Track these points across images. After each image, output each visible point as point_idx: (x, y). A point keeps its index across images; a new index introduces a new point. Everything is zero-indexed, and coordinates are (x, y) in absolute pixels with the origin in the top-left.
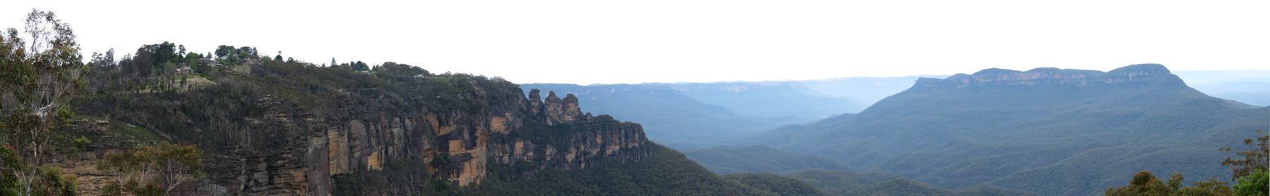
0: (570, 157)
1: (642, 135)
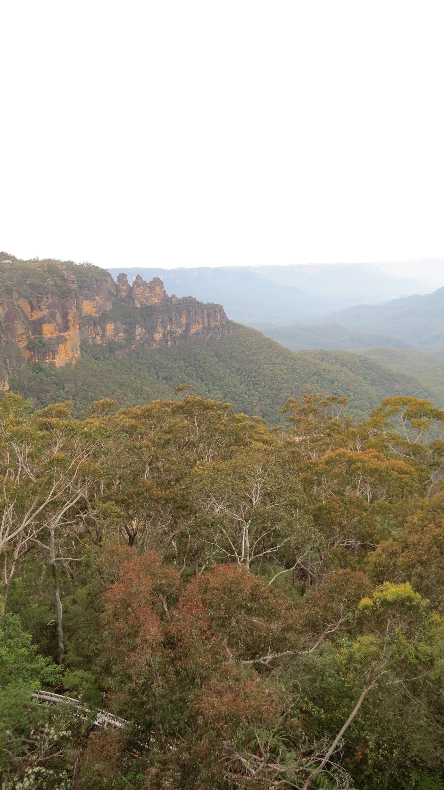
0: (158, 336)
1: (223, 315)
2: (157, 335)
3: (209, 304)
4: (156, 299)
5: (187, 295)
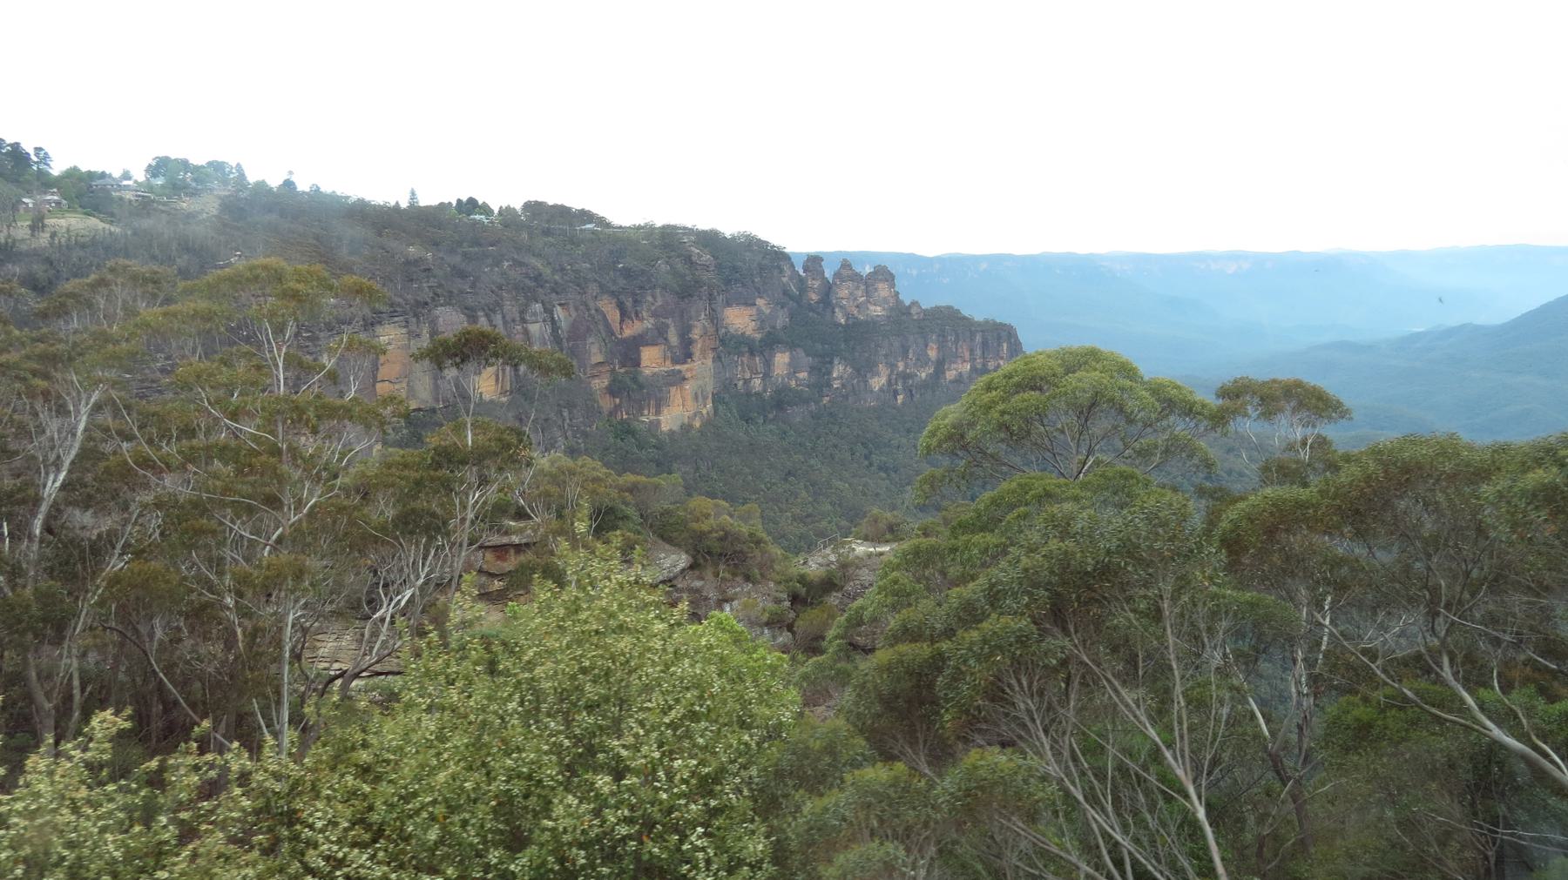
0: (878, 382)
3: (987, 322)
5: (943, 301)
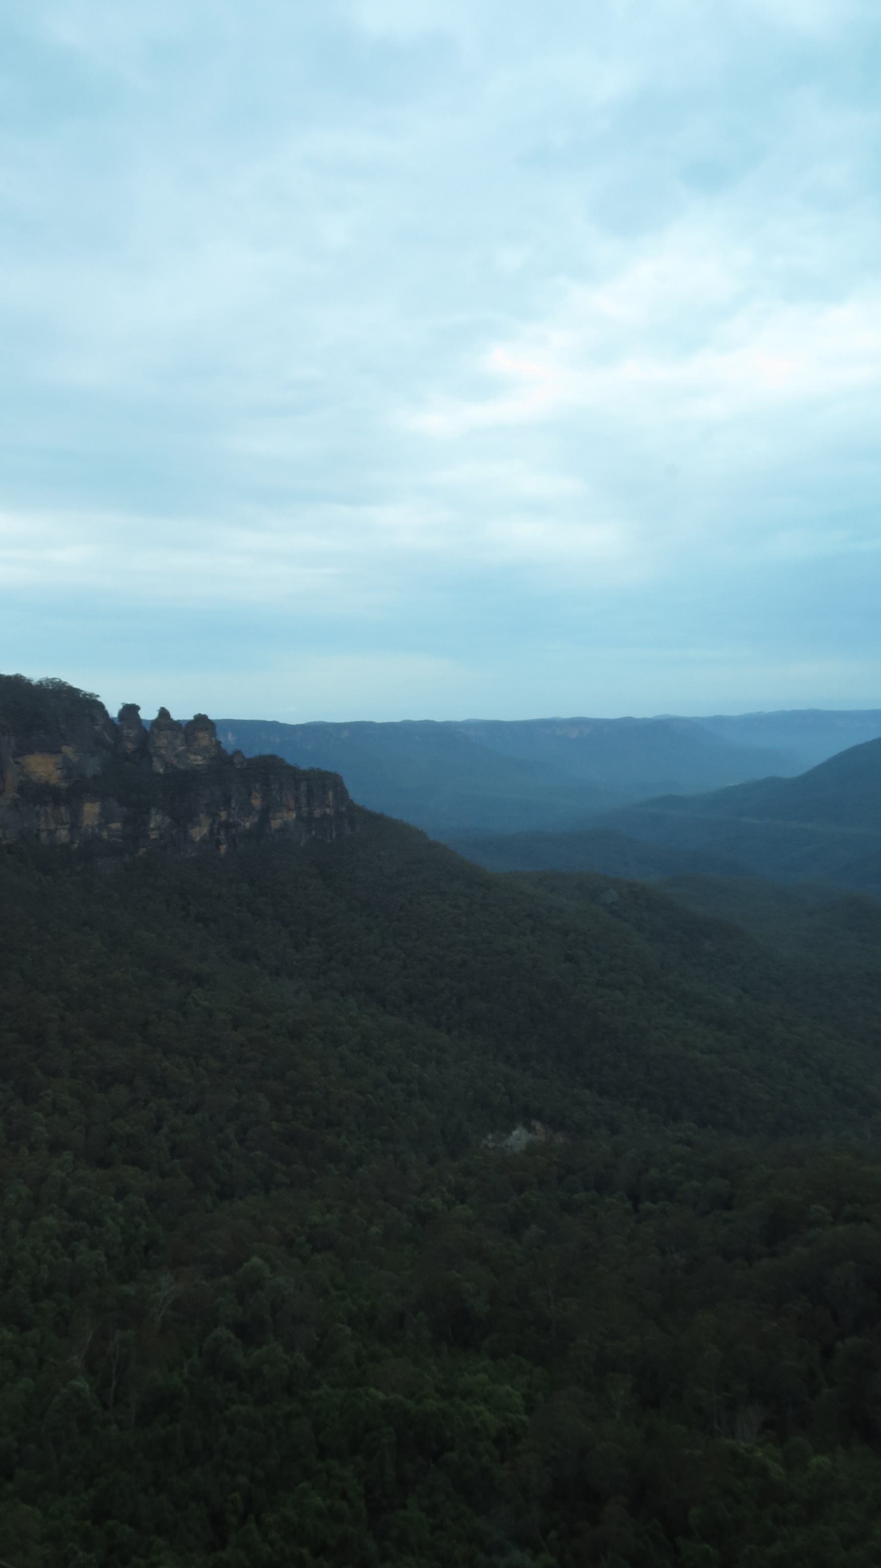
0: (199, 832)
2: (197, 829)
3: (312, 770)
4: (199, 758)
5: (267, 751)
